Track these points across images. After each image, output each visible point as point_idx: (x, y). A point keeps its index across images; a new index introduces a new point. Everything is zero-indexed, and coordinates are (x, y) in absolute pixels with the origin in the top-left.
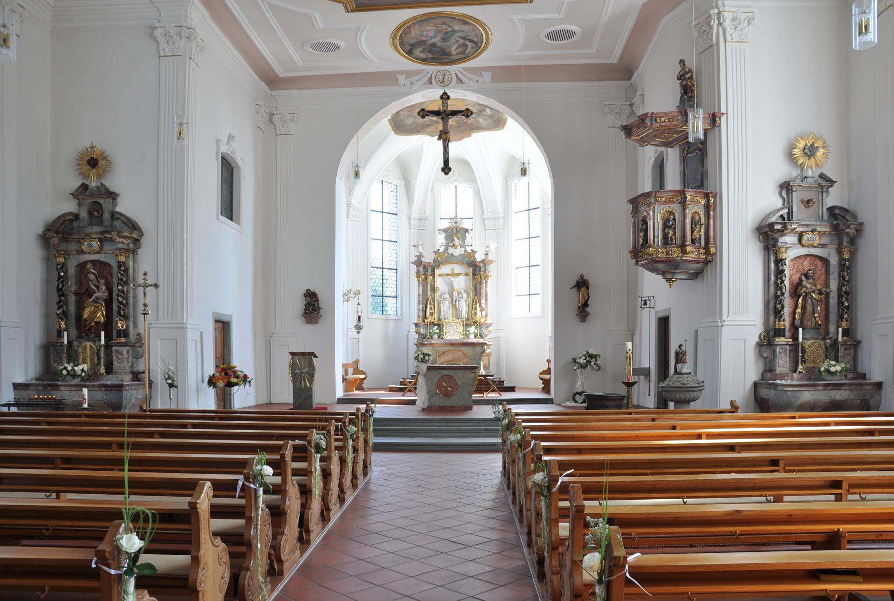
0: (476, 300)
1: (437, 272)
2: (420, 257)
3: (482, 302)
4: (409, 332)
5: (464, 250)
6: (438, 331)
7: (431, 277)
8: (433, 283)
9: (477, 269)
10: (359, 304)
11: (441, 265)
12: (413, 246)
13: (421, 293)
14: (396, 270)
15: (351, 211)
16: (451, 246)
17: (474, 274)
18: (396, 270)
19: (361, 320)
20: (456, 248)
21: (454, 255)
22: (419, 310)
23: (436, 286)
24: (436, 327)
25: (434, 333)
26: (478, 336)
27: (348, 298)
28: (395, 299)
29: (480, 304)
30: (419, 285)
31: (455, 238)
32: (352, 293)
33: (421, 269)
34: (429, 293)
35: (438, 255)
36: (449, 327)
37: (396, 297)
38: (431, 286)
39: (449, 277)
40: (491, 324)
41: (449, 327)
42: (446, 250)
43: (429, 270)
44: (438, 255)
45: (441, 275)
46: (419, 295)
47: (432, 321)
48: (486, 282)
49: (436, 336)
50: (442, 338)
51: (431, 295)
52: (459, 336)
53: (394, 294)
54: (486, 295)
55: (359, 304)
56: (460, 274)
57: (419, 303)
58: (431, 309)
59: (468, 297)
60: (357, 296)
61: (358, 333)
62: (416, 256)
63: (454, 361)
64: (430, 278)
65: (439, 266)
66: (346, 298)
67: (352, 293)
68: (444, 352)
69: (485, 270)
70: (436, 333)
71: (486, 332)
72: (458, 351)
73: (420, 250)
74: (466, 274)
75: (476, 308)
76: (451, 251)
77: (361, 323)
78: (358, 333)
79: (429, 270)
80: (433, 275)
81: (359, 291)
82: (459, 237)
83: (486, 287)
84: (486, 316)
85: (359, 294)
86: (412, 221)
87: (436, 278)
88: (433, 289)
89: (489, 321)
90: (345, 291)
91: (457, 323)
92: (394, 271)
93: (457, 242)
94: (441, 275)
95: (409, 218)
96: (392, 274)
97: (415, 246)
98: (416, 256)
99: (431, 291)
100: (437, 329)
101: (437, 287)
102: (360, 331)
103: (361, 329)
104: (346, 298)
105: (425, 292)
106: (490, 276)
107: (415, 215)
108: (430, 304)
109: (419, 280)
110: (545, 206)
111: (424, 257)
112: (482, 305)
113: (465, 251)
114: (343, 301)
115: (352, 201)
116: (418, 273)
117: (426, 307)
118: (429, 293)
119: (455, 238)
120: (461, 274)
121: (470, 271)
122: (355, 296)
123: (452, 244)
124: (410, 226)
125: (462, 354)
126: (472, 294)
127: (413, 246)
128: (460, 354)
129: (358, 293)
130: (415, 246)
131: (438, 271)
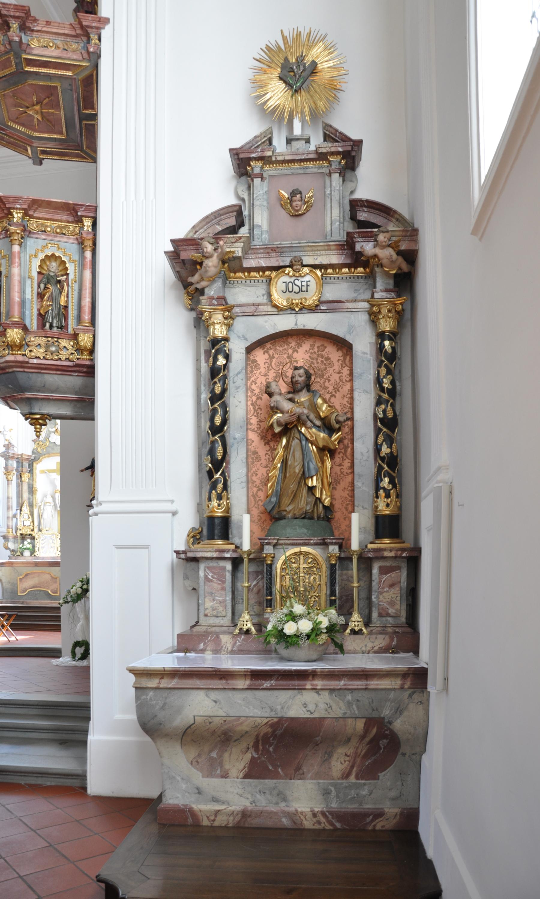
6: (30, 546)
24: (29, 540)
25: (24, 549)
34: (26, 495)
36: (42, 540)
38: (29, 487)
41: (42, 540)
47: (28, 533)
49: (27, 553)
50: (35, 556)
63: (40, 587)
64: (26, 477)
68: (27, 575)
70: (26, 549)
72: (45, 573)
88: (32, 490)
99: (29, 493)
100: (29, 543)
111: (15, 448)
116: (7, 471)
118: (26, 495)
125: (50, 578)
128: (47, 577)
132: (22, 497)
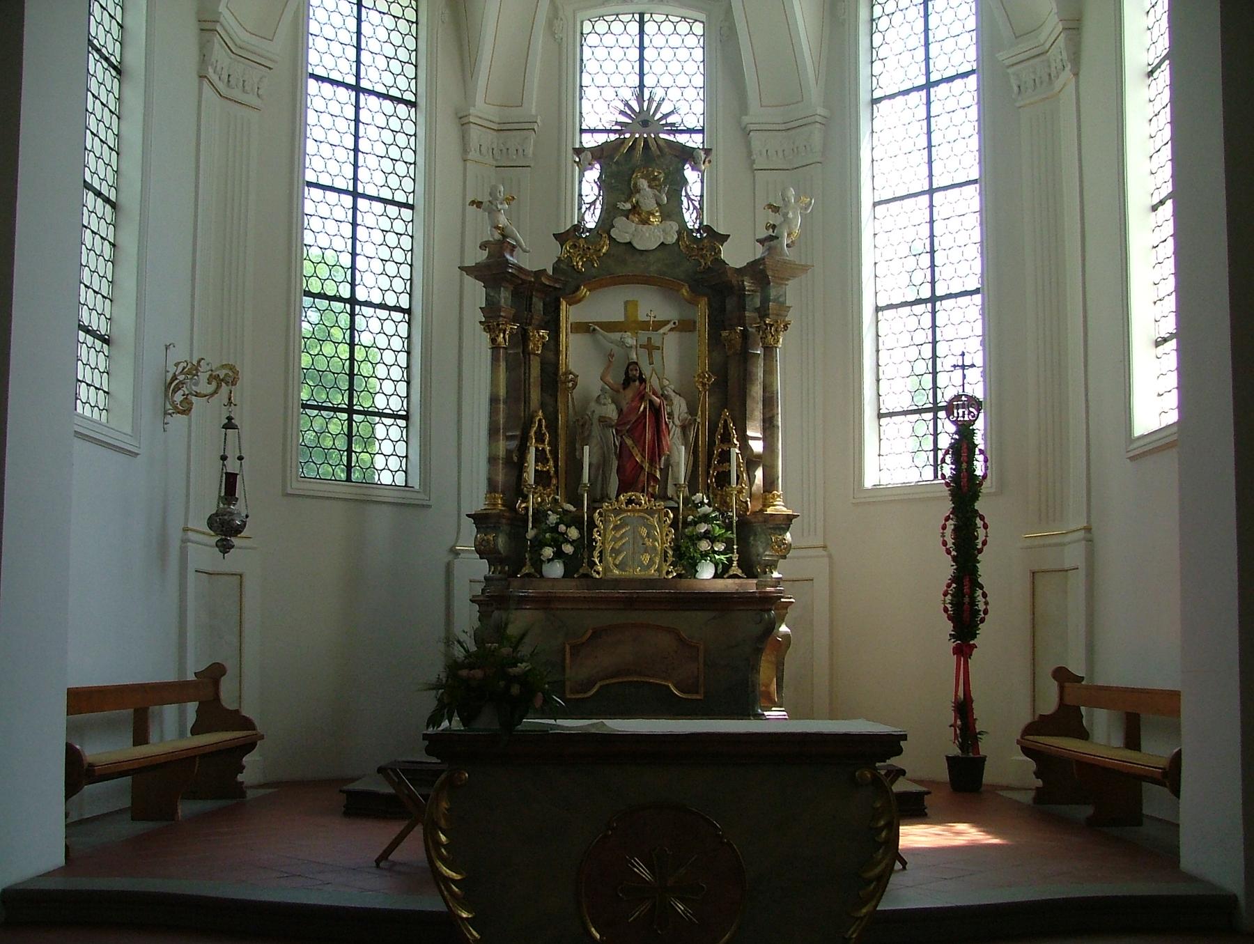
0: (726, 426)
1: (569, 314)
2: (500, 246)
3: (749, 433)
4: (457, 554)
5: (675, 227)
7: (542, 332)
8: (550, 355)
9: (731, 303)
10: (230, 425)
11: (583, 290)
12: (473, 203)
13: (502, 392)
14: (408, 311)
15: (219, 53)
16: (626, 214)
17: (718, 323)
18: (408, 311)
19: (239, 493)
20: (645, 222)
21: (639, 246)
22: (492, 460)
23: (562, 369)
26: (735, 570)
27: (186, 397)
28: (402, 423)
29: (744, 439)
30: (495, 360)
31: (644, 183)
32: (203, 377)
33: (504, 296)
34: (535, 395)
35: (574, 246)
36: (616, 528)
37: (406, 418)
39: (616, 336)
40: (789, 519)
41: (616, 528)
42: (606, 223)
43: (538, 305)
44: (574, 246)
45: (582, 328)
46: (494, 400)
48: (769, 350)
51: (543, 406)
52: (658, 570)
53: (396, 405)
54: (769, 402)
55: (230, 425)
56: (659, 325)
57: (493, 432)
58: (541, 457)
59: (692, 410)
60: (224, 389)
61: (225, 547)
62: (484, 246)
65: (578, 288)
66: (178, 397)
67: (203, 377)
68: (597, 634)
69: (765, 300)
71: (768, 556)
73: (503, 220)
74: (685, 326)
75: (725, 457)
76: (624, 230)
77: (239, 507)
78: (225, 547)
79: (538, 305)
80: (553, 325)
81: (232, 368)
82: (655, 178)
83: (769, 371)
84: (769, 484)
85: (234, 383)
86: (475, 133)
87: (563, 337)
89: (779, 507)
90: (172, 370)
91: (651, 512)
92: (397, 316)
93: (648, 197)
94: (582, 328)
95: (463, 122)
96: (389, 327)
97: (479, 204)
98: (484, 246)
101: (568, 372)
102: (235, 541)
103: (237, 531)
104: (178, 397)
105: (517, 391)
106: (786, 328)
107: (482, 108)
108: (540, 439)
109: (493, 340)
110: (1001, 56)
111: (518, 251)
112: (751, 443)
113: (679, 233)
114: (166, 413)
115: (222, 8)
117: (523, 450)
119: (644, 183)
120: (668, 322)
121: (701, 312)
122: (215, 392)
123: (628, 206)
124: (465, 150)
126: (706, 400)
127: (473, 203)
129: (226, 378)
130: (479, 204)
131: (572, 308)
132: (527, 401)
